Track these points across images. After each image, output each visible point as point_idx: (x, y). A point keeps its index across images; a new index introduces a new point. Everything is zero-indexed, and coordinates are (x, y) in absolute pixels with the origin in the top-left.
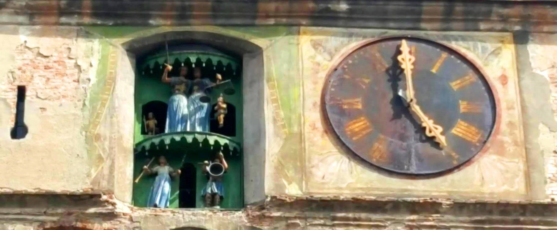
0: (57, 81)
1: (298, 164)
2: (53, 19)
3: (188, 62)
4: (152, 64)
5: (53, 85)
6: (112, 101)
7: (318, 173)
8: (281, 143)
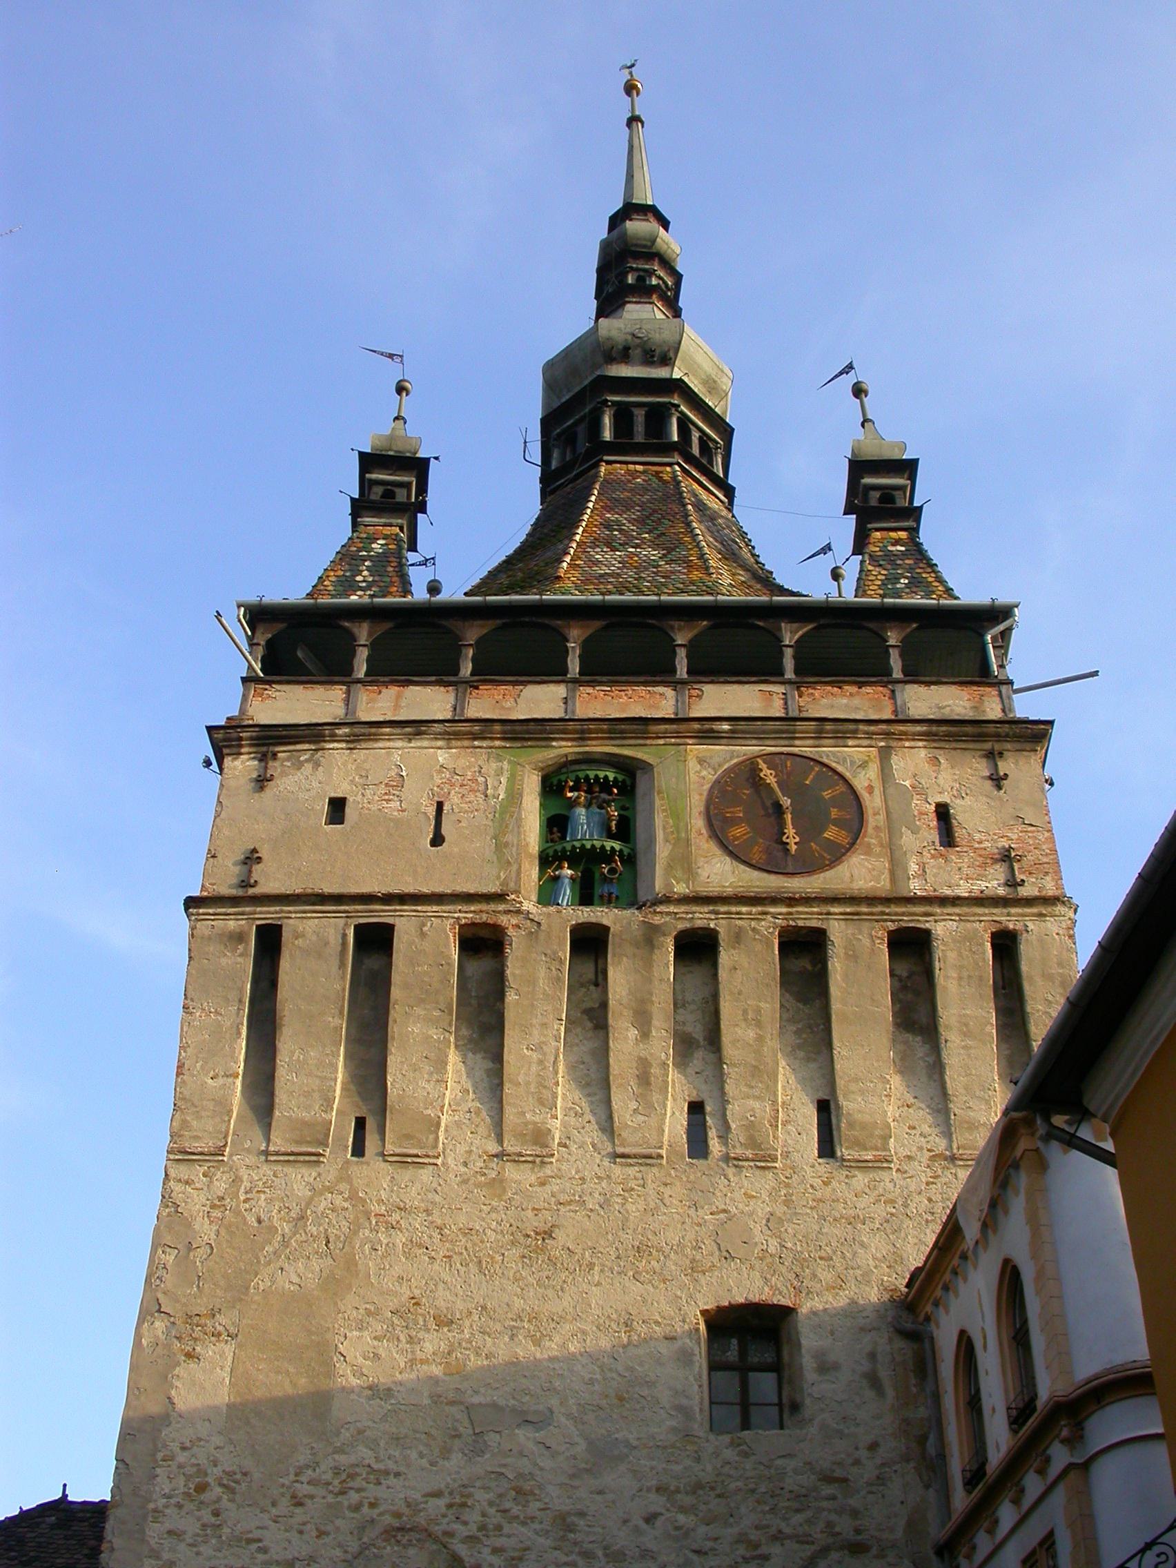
0: (471, 797)
1: (686, 865)
2: (466, 743)
3: (587, 778)
4: (555, 782)
5: (467, 800)
6: (520, 813)
8: (670, 847)
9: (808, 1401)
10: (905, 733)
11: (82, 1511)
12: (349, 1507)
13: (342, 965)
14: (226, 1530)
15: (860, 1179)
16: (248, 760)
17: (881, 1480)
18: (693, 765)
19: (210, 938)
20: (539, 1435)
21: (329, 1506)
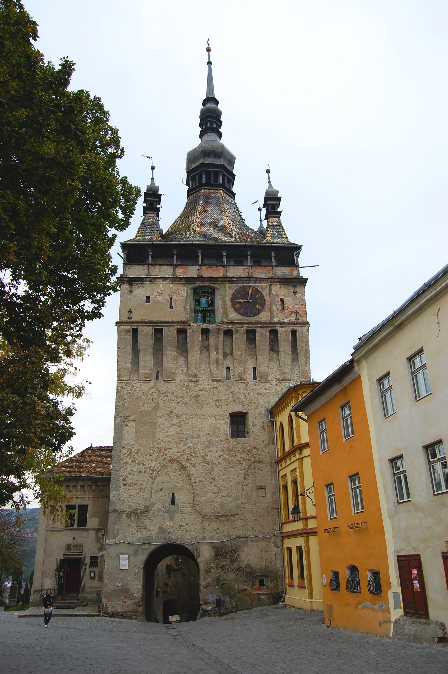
2: (176, 282)
7: (230, 316)
9: (250, 432)
10: (275, 281)
11: (96, 449)
12: (161, 456)
13: (152, 338)
14: (137, 461)
15: (262, 385)
16: (127, 285)
17: (265, 448)
18: (227, 289)
19: (122, 331)
20: (198, 440)
21: (157, 455)
